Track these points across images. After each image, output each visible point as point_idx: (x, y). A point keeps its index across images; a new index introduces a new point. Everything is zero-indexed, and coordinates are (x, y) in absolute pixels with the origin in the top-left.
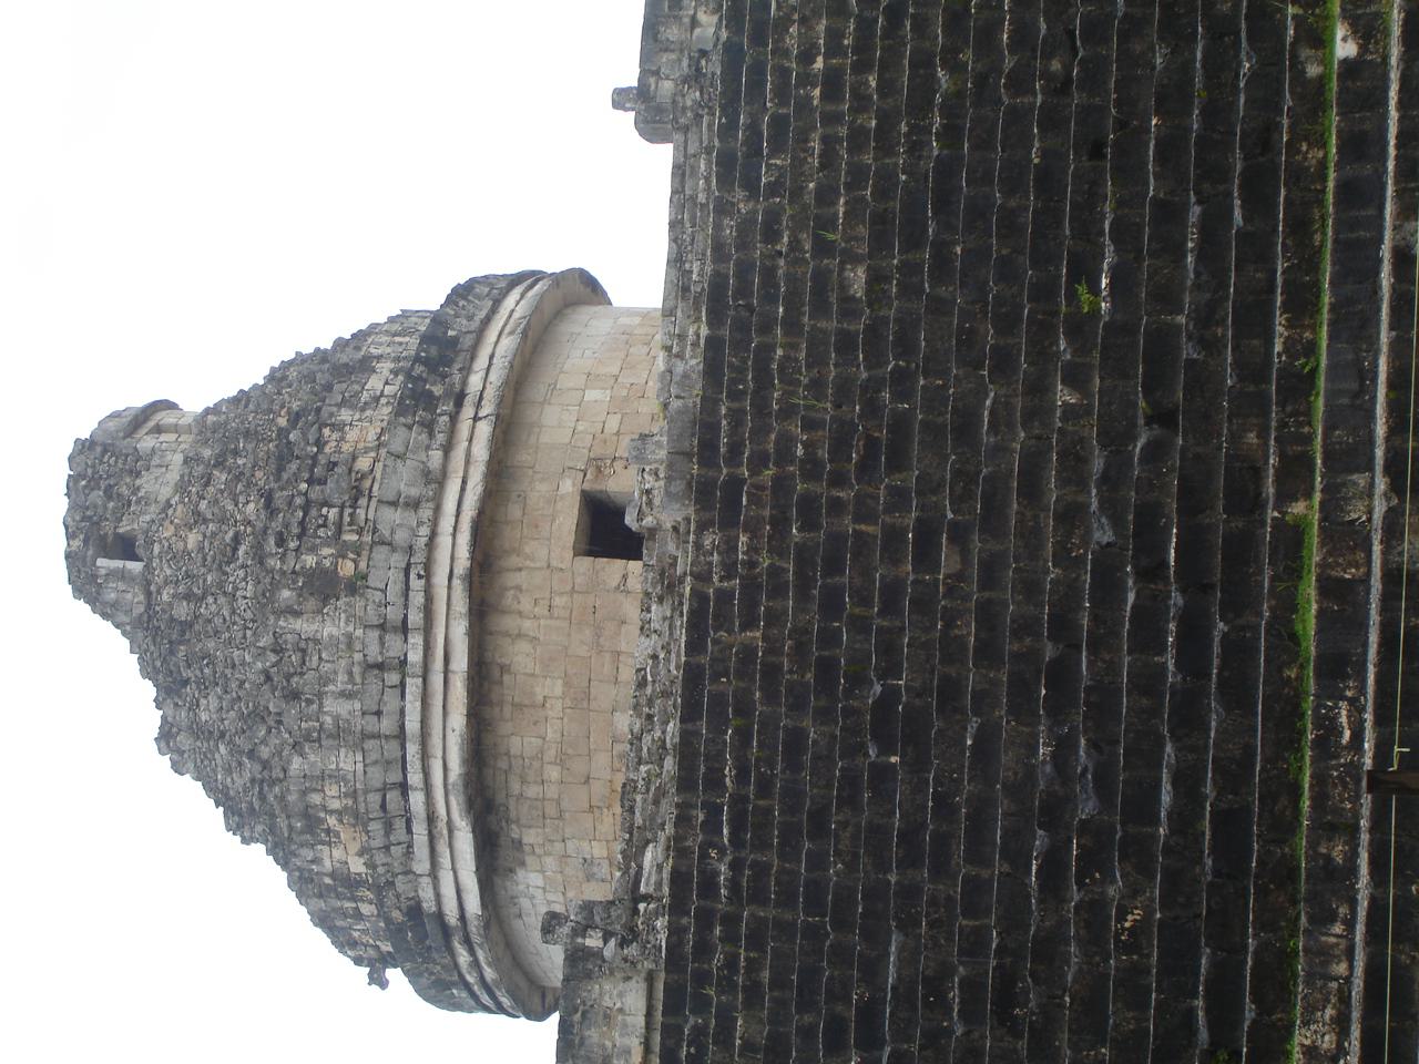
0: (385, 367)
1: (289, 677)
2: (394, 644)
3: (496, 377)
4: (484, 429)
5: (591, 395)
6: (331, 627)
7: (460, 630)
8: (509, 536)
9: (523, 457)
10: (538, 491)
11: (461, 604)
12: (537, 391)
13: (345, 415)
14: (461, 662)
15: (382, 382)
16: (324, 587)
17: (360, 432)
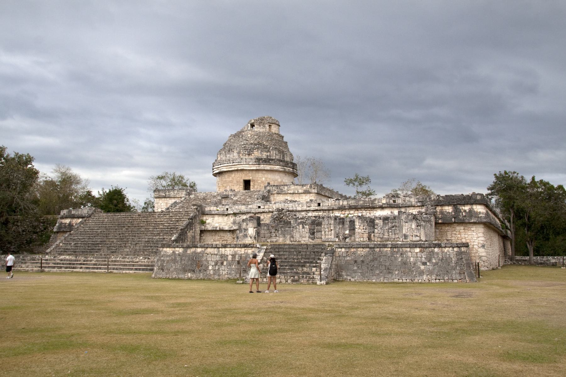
0: (268, 154)
1: (230, 151)
2: (232, 162)
3: (263, 168)
4: (255, 168)
5: (264, 179)
6: (235, 154)
7: (233, 169)
8: (245, 172)
9: (254, 172)
10: (250, 175)
11: (236, 169)
12: (264, 172)
13: (259, 151)
14: (230, 169)
15: (264, 155)
16: (239, 153)
17: (257, 154)
